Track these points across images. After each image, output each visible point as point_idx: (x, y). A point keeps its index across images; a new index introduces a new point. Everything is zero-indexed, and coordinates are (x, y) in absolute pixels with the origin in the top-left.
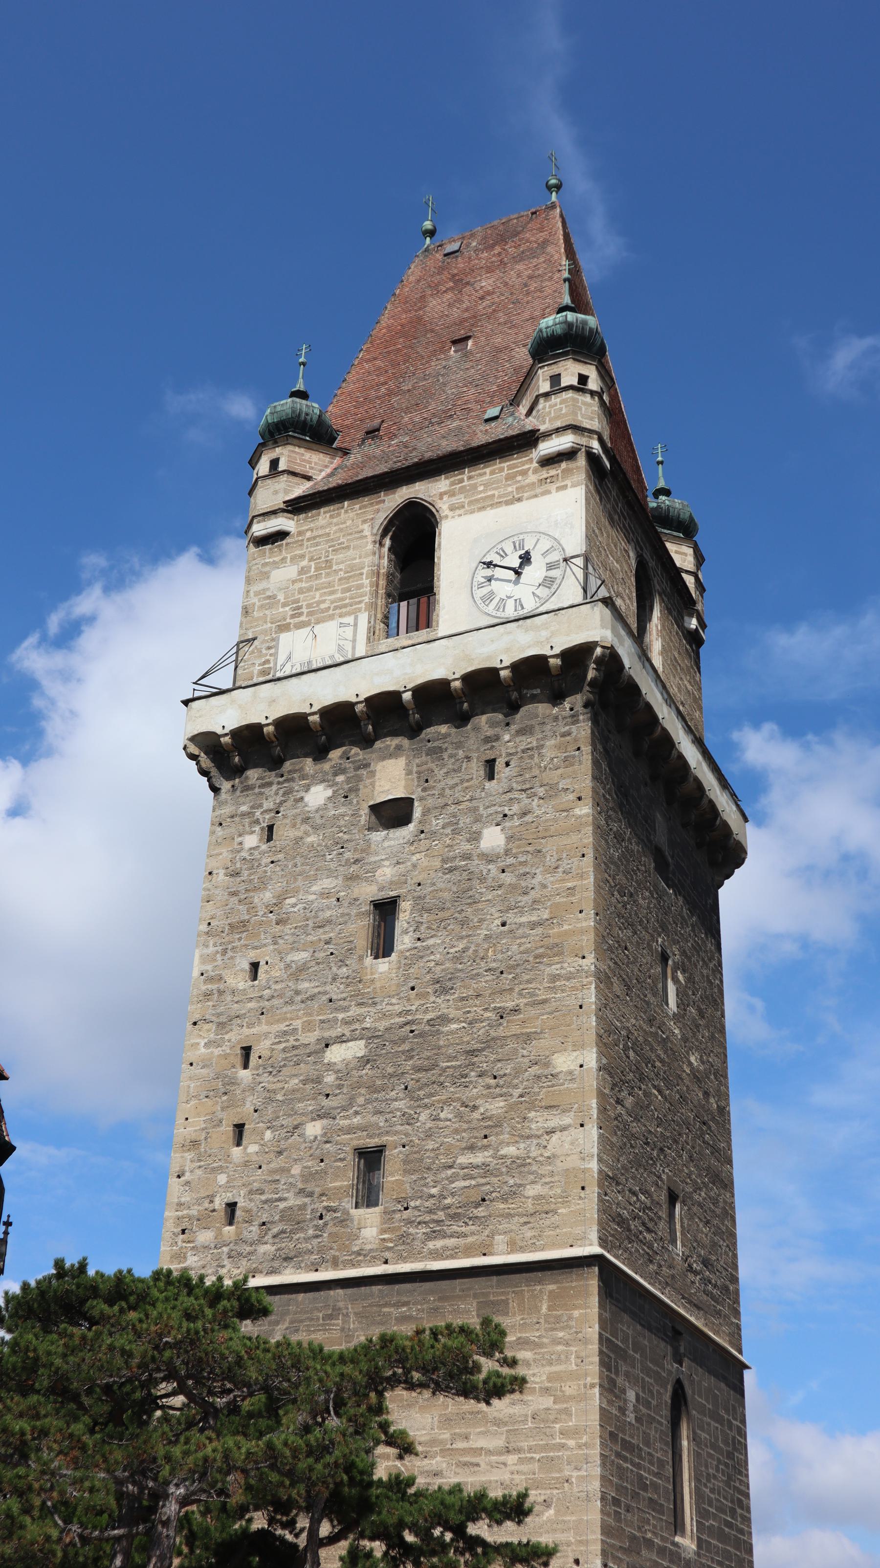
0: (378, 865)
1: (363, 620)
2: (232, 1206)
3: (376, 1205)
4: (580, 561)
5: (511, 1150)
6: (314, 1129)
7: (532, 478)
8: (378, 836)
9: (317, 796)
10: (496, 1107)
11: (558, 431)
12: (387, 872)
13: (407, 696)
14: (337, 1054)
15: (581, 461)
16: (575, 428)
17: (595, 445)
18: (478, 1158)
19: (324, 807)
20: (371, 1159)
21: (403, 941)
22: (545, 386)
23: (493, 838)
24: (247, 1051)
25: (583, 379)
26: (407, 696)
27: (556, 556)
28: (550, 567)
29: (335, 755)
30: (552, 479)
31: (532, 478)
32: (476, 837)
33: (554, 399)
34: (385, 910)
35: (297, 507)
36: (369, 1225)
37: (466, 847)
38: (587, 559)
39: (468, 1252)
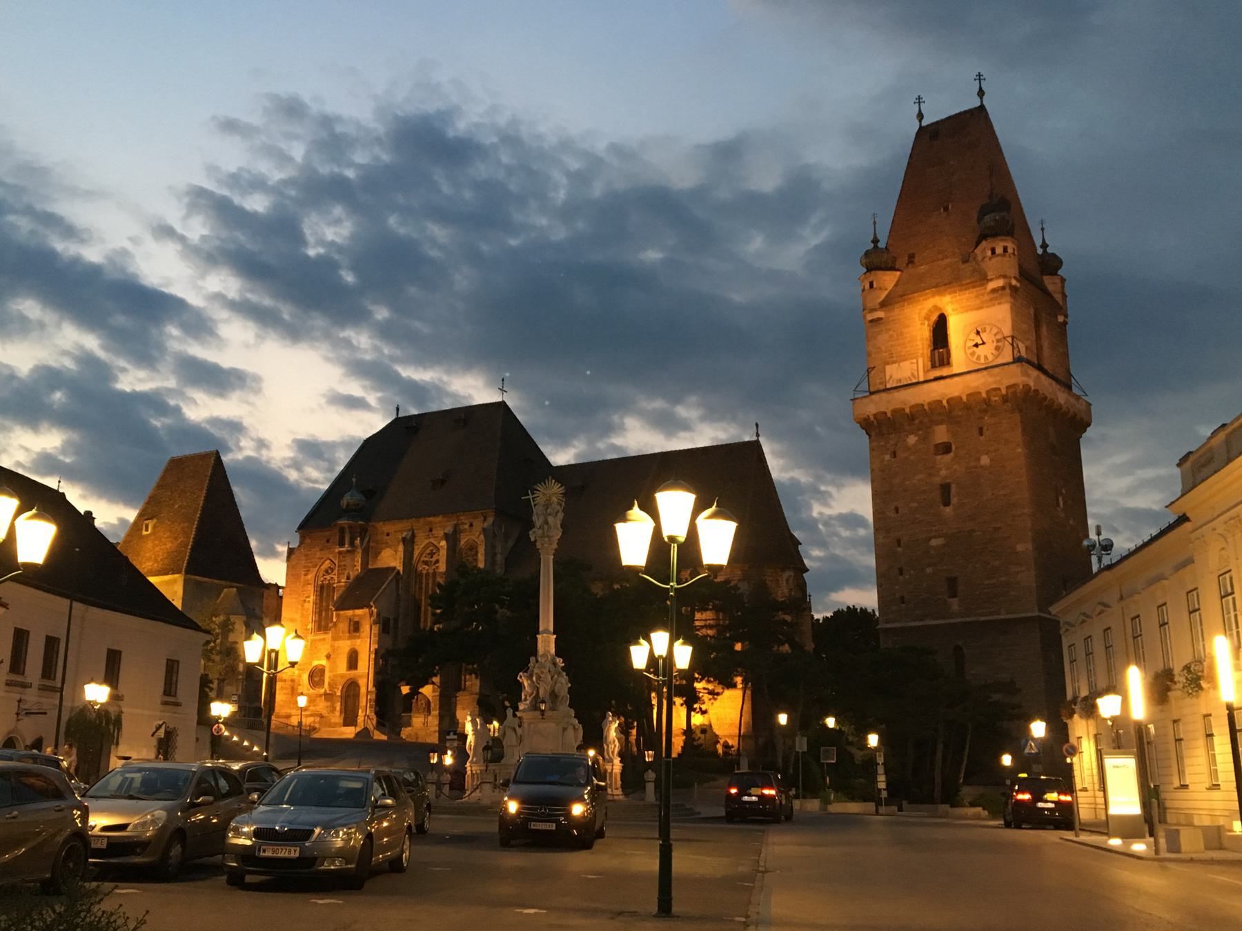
0: (940, 469)
1: (921, 361)
2: (902, 600)
3: (955, 596)
4: (1010, 340)
5: (1003, 579)
6: (929, 570)
7: (987, 297)
8: (939, 457)
9: (912, 440)
10: (997, 563)
11: (998, 277)
12: (943, 472)
13: (945, 402)
14: (934, 542)
15: (1008, 291)
16: (1004, 277)
17: (1014, 282)
18: (993, 581)
19: (915, 445)
20: (952, 583)
21: (954, 500)
22: (989, 253)
23: (985, 460)
24: (899, 542)
25: (1005, 249)
26: (945, 402)
27: (999, 337)
28: (998, 341)
29: (917, 422)
30: (996, 299)
31: (987, 297)
32: (979, 459)
33: (994, 260)
34: (945, 489)
35: (884, 305)
36: (955, 604)
37: (973, 464)
38: (1013, 338)
39: (991, 614)
